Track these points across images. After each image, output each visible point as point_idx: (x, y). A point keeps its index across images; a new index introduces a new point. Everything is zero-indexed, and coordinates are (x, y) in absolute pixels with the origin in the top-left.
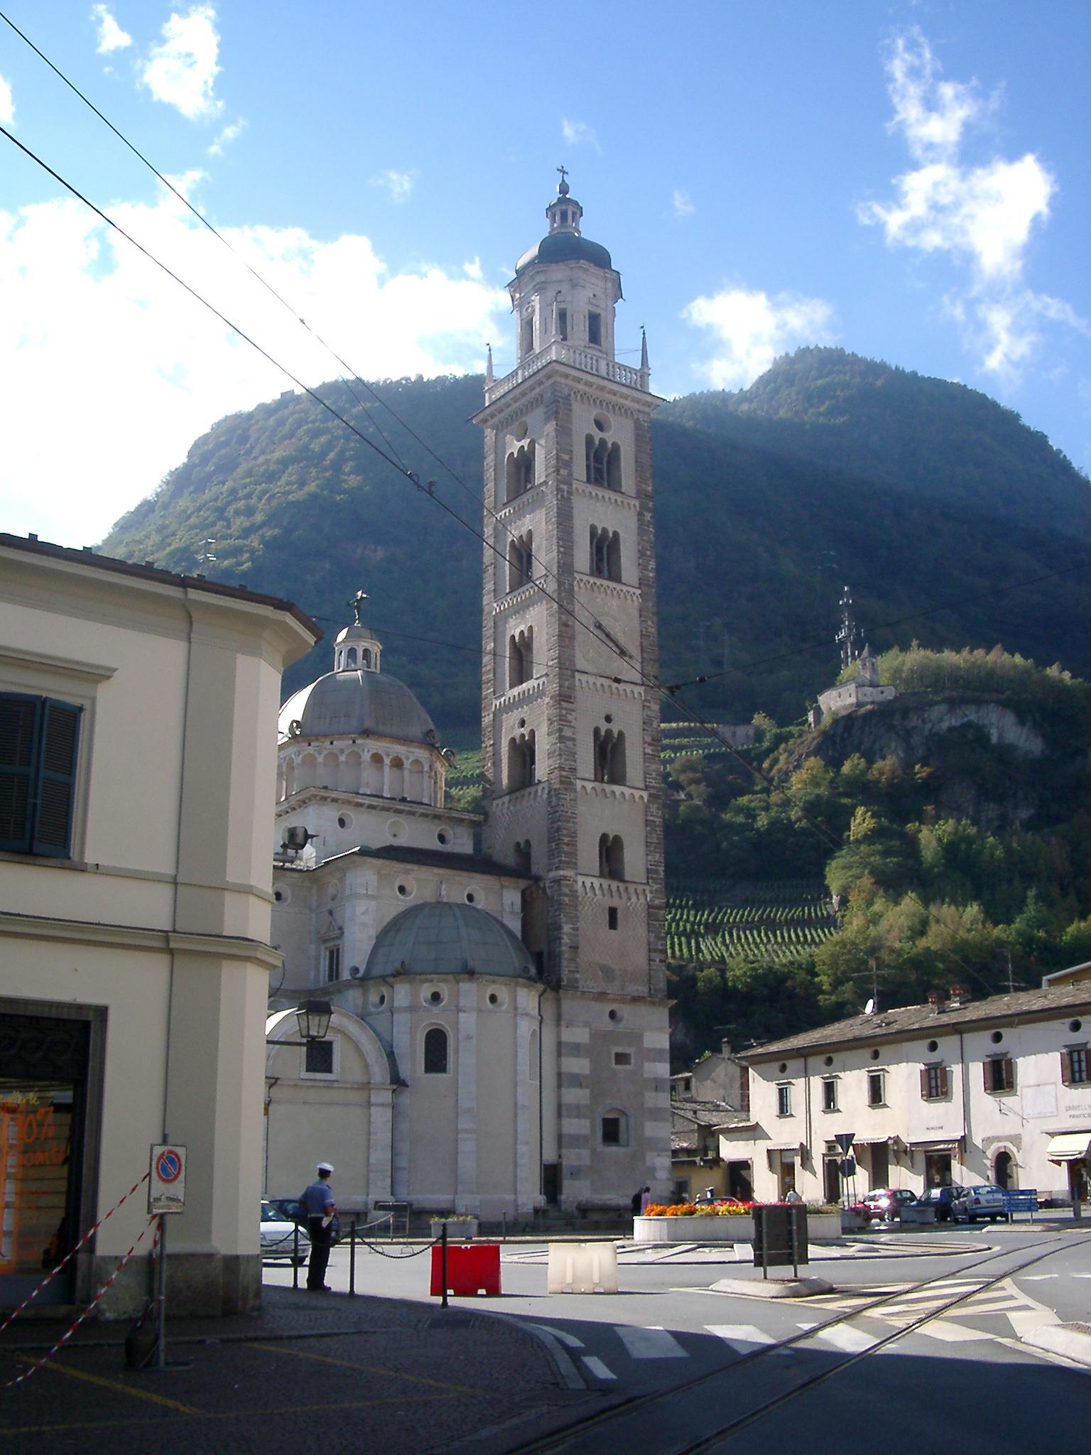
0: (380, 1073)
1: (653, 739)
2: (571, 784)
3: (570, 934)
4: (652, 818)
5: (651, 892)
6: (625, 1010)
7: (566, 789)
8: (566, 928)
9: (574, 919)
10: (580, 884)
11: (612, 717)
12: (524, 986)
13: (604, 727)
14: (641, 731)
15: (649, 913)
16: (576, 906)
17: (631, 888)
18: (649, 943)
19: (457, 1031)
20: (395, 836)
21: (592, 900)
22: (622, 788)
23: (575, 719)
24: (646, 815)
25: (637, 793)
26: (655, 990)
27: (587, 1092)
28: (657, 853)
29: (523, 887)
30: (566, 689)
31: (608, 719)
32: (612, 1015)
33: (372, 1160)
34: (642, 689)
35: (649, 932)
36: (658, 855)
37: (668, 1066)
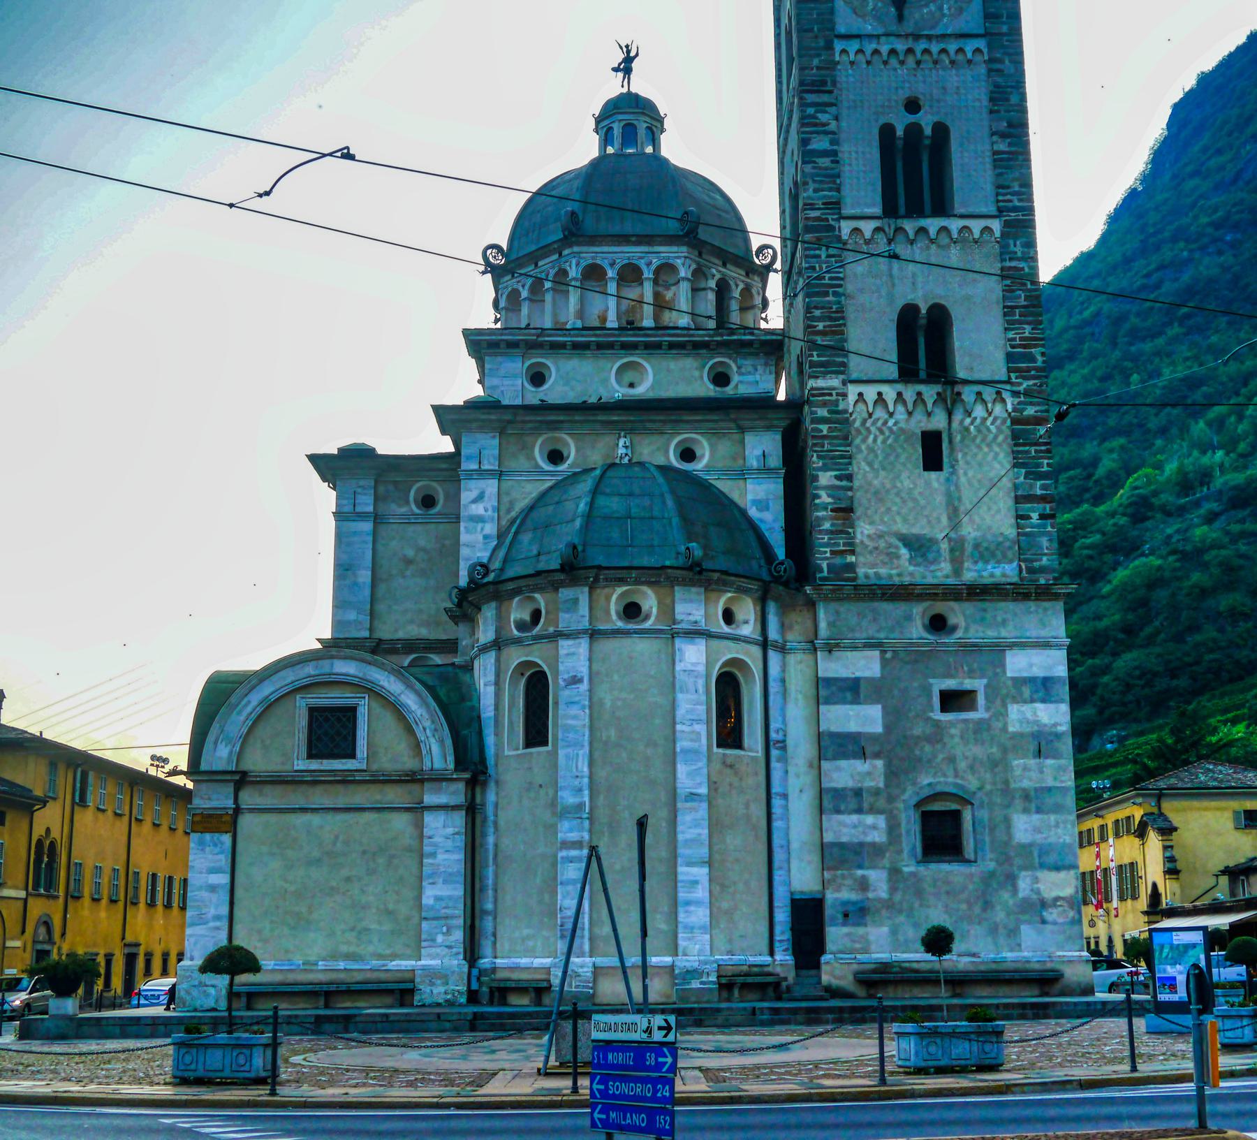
0: (438, 755)
1: (1010, 125)
2: (832, 228)
4: (1013, 264)
5: (1016, 394)
6: (957, 614)
8: (826, 478)
9: (842, 463)
10: (852, 398)
11: (921, 103)
12: (691, 583)
14: (985, 115)
15: (1013, 431)
16: (846, 438)
17: (968, 394)
18: (1016, 487)
19: (556, 673)
20: (632, 385)
21: (885, 423)
23: (837, 118)
24: (1002, 260)
25: (976, 226)
26: (1031, 571)
27: (879, 763)
28: (1029, 323)
29: (784, 424)
31: (912, 106)
32: (938, 624)
33: (427, 900)
34: (981, 44)
35: (1014, 466)
36: (1028, 328)
37: (1065, 708)
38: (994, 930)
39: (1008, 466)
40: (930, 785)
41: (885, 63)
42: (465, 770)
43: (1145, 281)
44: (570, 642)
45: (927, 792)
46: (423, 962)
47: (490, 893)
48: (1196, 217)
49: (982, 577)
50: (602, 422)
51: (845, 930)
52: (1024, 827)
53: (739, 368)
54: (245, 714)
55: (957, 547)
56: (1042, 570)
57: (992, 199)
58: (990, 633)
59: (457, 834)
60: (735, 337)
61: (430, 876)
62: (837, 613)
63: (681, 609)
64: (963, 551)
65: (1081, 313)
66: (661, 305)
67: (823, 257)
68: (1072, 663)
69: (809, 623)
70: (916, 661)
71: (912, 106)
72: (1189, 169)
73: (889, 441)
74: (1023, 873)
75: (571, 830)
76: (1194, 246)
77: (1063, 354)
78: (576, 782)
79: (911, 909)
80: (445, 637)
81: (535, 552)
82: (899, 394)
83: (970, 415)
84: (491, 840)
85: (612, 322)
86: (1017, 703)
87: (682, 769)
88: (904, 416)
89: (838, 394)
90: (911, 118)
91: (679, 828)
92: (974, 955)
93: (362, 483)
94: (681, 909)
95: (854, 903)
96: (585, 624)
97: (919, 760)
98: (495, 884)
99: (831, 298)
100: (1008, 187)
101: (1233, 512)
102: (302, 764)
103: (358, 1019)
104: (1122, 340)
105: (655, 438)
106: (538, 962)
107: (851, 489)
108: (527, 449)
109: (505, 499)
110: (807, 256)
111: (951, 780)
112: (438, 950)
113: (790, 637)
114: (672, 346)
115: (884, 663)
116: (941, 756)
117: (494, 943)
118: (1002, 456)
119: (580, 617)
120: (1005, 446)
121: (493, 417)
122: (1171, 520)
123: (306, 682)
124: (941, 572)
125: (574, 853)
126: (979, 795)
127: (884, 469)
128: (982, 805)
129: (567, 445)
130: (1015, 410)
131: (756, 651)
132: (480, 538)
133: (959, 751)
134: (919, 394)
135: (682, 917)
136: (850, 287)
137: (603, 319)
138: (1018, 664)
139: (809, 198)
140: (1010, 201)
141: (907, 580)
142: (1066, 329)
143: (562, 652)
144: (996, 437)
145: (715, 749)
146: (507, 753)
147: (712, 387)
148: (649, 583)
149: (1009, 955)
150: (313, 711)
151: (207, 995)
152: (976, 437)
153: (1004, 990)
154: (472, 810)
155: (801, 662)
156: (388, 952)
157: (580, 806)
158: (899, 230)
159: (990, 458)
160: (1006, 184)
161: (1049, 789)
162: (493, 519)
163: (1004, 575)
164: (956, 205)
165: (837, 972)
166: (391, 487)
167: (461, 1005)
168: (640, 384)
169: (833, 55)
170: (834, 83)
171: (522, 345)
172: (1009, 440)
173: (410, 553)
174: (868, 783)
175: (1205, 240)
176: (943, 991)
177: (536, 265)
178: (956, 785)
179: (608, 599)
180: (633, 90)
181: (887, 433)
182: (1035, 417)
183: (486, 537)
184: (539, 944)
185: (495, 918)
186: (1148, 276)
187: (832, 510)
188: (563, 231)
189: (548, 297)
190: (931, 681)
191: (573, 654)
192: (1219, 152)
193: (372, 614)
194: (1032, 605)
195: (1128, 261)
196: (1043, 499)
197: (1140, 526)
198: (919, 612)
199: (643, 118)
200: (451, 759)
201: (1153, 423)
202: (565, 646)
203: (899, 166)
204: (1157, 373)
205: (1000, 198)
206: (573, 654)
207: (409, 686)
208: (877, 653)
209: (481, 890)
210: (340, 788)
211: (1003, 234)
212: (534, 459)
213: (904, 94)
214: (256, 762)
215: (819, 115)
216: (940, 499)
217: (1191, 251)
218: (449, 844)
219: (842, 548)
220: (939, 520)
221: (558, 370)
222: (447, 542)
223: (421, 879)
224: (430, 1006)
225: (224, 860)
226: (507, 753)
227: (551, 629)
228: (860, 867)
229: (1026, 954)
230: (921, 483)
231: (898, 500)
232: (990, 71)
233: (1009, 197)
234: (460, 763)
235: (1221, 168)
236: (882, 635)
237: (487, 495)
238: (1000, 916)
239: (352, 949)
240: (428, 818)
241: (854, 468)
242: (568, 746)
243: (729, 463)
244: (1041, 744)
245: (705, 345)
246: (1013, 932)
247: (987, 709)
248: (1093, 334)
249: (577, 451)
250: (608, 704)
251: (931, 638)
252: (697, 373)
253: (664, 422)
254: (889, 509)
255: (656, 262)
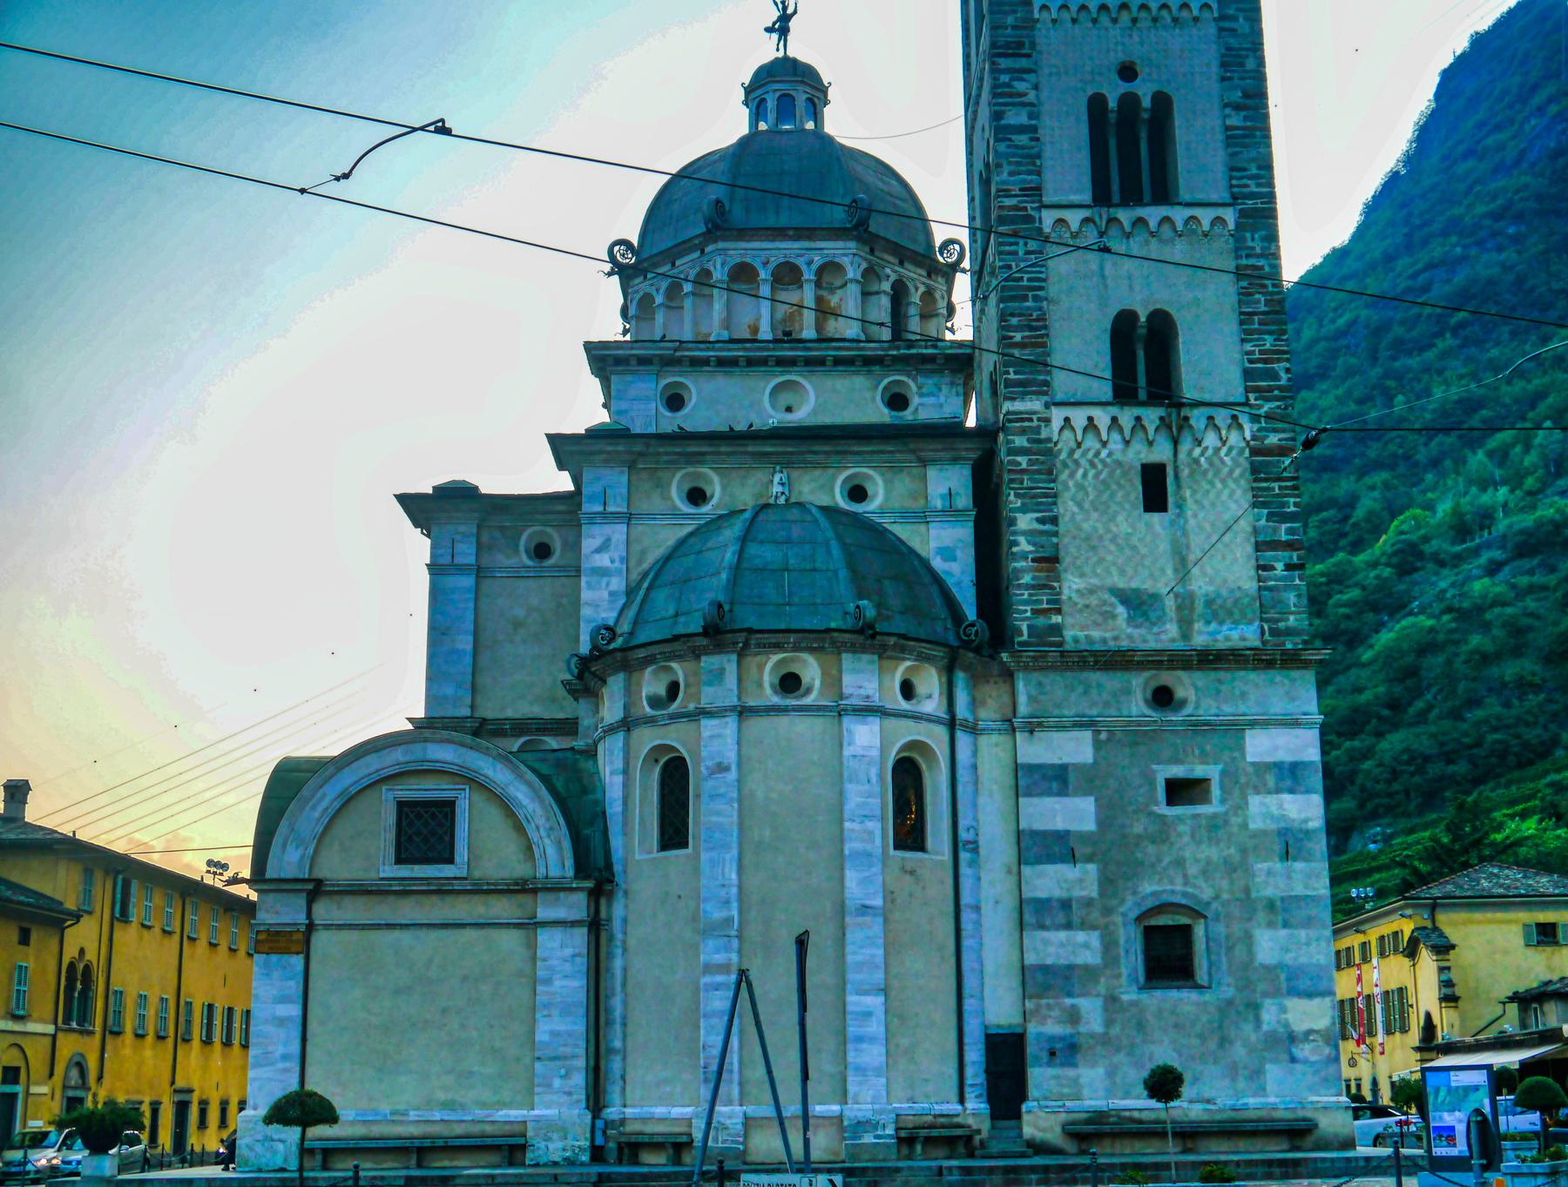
0: (555, 858)
1: (1246, 95)
2: (1029, 219)
3: (1029, 533)
4: (1251, 262)
5: (1255, 418)
6: (1186, 685)
7: (1015, 234)
8: (1025, 522)
9: (1045, 503)
10: (1057, 423)
12: (864, 649)
13: (1114, 92)
15: (1252, 464)
16: (1050, 472)
17: (1197, 418)
18: (1256, 531)
19: (698, 761)
20: (789, 409)
21: (1097, 454)
22: (1164, 211)
23: (1036, 87)
24: (1238, 257)
25: (1206, 216)
26: (1274, 632)
27: (1092, 868)
28: (1270, 333)
29: (974, 455)
30: (1009, 31)
31: (1128, 72)
32: (1163, 698)
35: (1254, 505)
37: (1317, 799)
38: (1233, 1071)
39: (1246, 506)
40: (1154, 894)
41: (1095, 21)
42: (587, 877)
43: (1410, 283)
44: (714, 722)
45: (1149, 904)
46: (536, 1112)
47: (618, 1028)
48: (1470, 207)
49: (1216, 640)
50: (754, 454)
51: (1052, 1071)
52: (1269, 945)
53: (920, 388)
54: (320, 809)
55: (1186, 604)
56: (1289, 632)
57: (1224, 184)
58: (1227, 709)
59: (574, 955)
60: (914, 351)
61: (547, 1006)
62: (1040, 684)
63: (849, 681)
64: (1192, 609)
65: (1333, 321)
66: (824, 311)
67: (1021, 253)
68: (1326, 746)
69: (1006, 699)
70: (1137, 744)
71: (1128, 72)
72: (1461, 148)
73: (1102, 477)
74: (1268, 1001)
75: (717, 951)
76: (1468, 241)
77: (1312, 371)
78: (723, 893)
79: (1133, 1045)
80: (561, 716)
81: (671, 612)
82: (1114, 420)
83: (1200, 444)
84: (618, 963)
85: (765, 333)
86: (1258, 793)
87: (851, 878)
88: (1120, 446)
89: (1039, 419)
90: (1125, 87)
91: (849, 949)
92: (1208, 1101)
93: (462, 528)
94: (850, 1046)
95: (1062, 1038)
96: (734, 701)
97: (1142, 864)
98: (624, 1018)
99: (1030, 304)
100: (1245, 170)
101: (1517, 563)
102: (391, 871)
103: (458, 1181)
104: (1383, 354)
105: (818, 472)
106: (677, 1112)
107: (1056, 534)
108: (662, 486)
109: (636, 548)
110: (1000, 253)
111: (1179, 888)
112: (555, 1098)
113: (982, 714)
114: (838, 361)
115: (1098, 745)
116: (1167, 860)
117: (624, 1089)
118: (1239, 492)
119: (724, 693)
120: (1243, 482)
121: (620, 448)
122: (1445, 572)
123: (391, 771)
124: (1167, 635)
125: (719, 978)
126: (1214, 905)
127: (1096, 510)
128: (1217, 919)
129: (711, 482)
130: (1254, 438)
131: (942, 732)
132: (606, 594)
133: (1187, 854)
134: (1138, 419)
135: (851, 1056)
136: (1053, 290)
137: (755, 329)
138: (1260, 746)
139: (1003, 182)
140: (1247, 186)
141: (1125, 644)
142: (1315, 341)
143: (706, 733)
144: (1231, 472)
145: (892, 851)
146: (637, 857)
147: (886, 411)
148: (811, 650)
149: (1252, 1101)
150: (402, 805)
151: (275, 1152)
152: (1205, 473)
153: (1243, 1144)
154: (596, 926)
155: (997, 745)
156: (495, 1099)
157: (728, 921)
158: (1112, 220)
159: (1224, 496)
160: (1245, 165)
161: (1299, 898)
162: (619, 572)
163: (1244, 639)
164: (1181, 192)
165: (1041, 1123)
166: (497, 534)
167: (583, 1164)
168: (799, 409)
169: (1032, 12)
170: (1033, 45)
171: (656, 361)
172: (1248, 475)
173: (520, 612)
174: (1078, 893)
175: (1483, 233)
176: (1171, 1145)
177: (673, 264)
178: (1185, 894)
179: (761, 668)
180: (791, 54)
181: (1100, 466)
182: (1280, 447)
183: (611, 594)
184: (678, 1089)
185: (624, 1058)
186: (1414, 276)
187: (1034, 560)
188: (706, 224)
189: (688, 303)
190: (1155, 767)
191: (719, 736)
192: (1498, 128)
193: (474, 689)
194: (1277, 676)
195: (1389, 259)
196: (1289, 546)
197: (1407, 579)
198: (1139, 684)
199: (801, 88)
200: (569, 863)
201: (1422, 455)
202: (708, 726)
203: (1112, 143)
204: (1427, 393)
205: (1234, 182)
206: (719, 736)
207: (520, 776)
208: (1087, 735)
209: (607, 1023)
210: (435, 899)
211: (1238, 226)
212: (670, 499)
213: (1120, 56)
214: (334, 868)
215: (1016, 83)
216: (1164, 546)
217: (1465, 247)
218: (568, 967)
219: (1045, 606)
220: (1163, 570)
221: (699, 392)
222: (565, 601)
223: (534, 1010)
224: (545, 1165)
225: (295, 987)
226: (637, 857)
227: (691, 706)
228: (1070, 995)
229: (1272, 1099)
230: (1141, 526)
231: (1112, 547)
232: (1221, 30)
233: (1245, 181)
234: (581, 869)
235: (1501, 147)
236: (1094, 712)
237: (614, 540)
238: (1239, 1052)
239: (450, 1096)
240: (545, 938)
241: (1060, 509)
242: (712, 849)
243: (909, 504)
244: (1289, 844)
245: (878, 361)
246: (1257, 1074)
247: (1223, 801)
248: (1348, 347)
249: (724, 488)
250: (760, 795)
251: (1155, 715)
252: (868, 395)
253: (827, 453)
254: (1101, 560)
255: (818, 260)
